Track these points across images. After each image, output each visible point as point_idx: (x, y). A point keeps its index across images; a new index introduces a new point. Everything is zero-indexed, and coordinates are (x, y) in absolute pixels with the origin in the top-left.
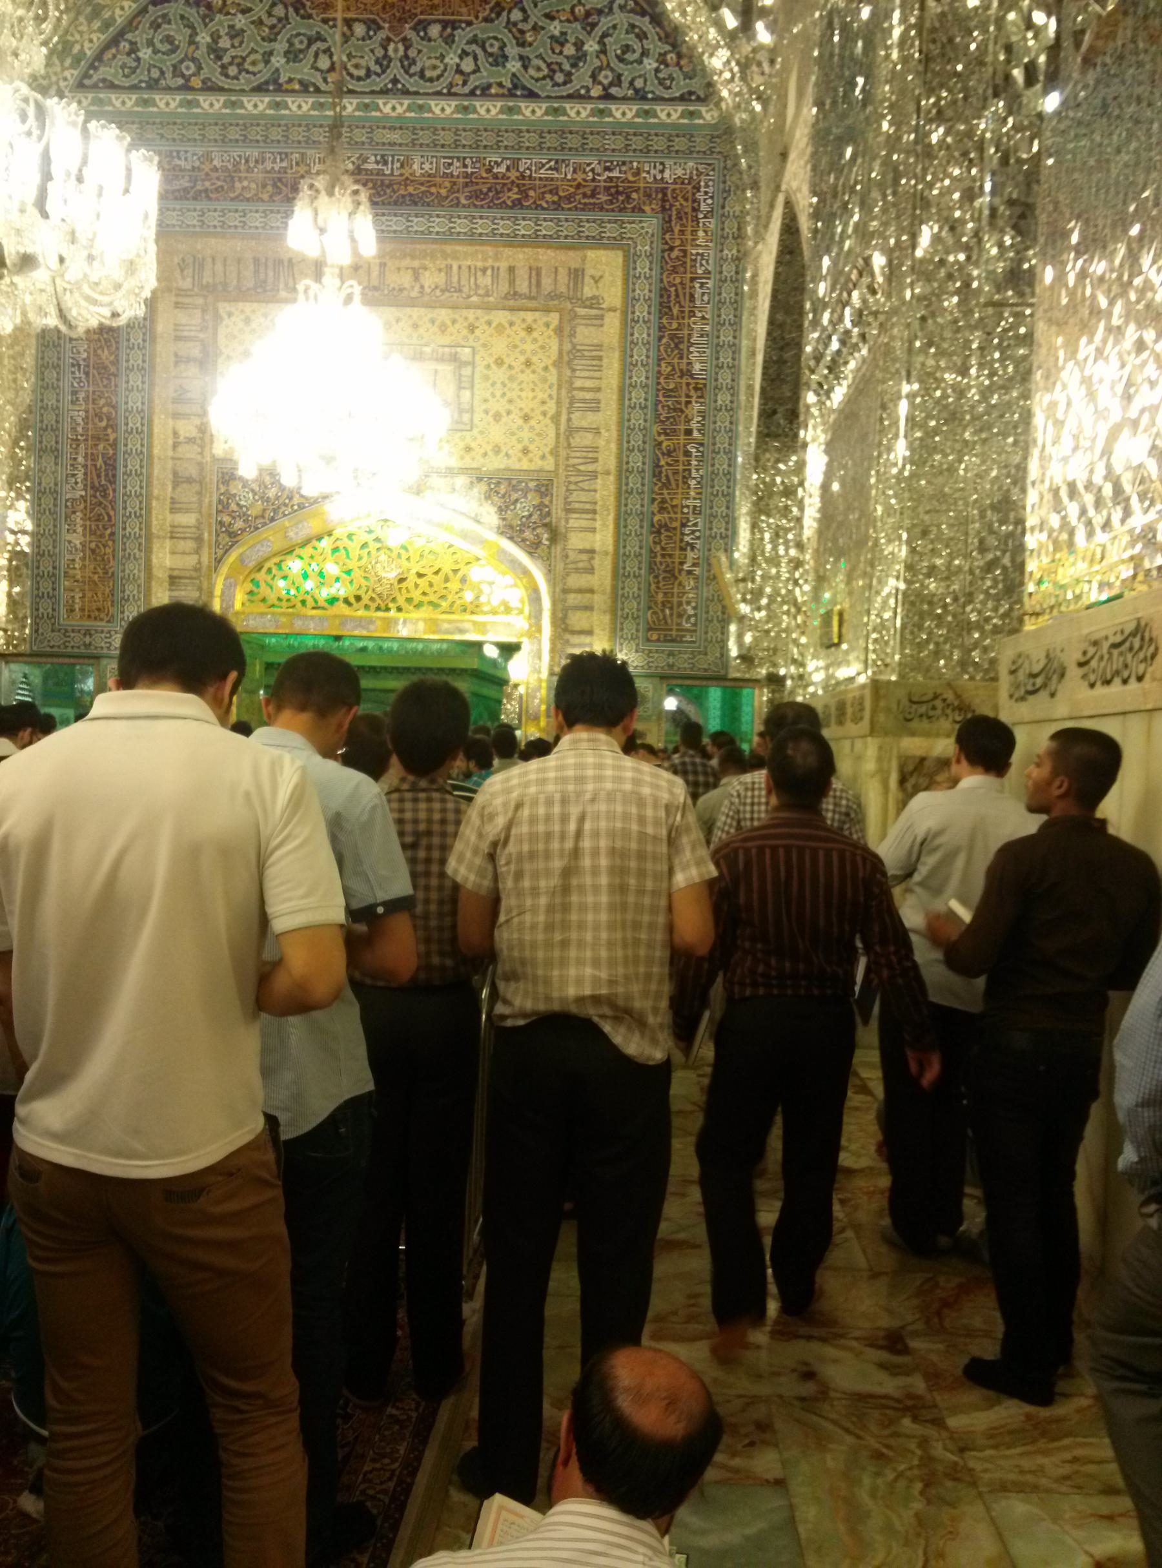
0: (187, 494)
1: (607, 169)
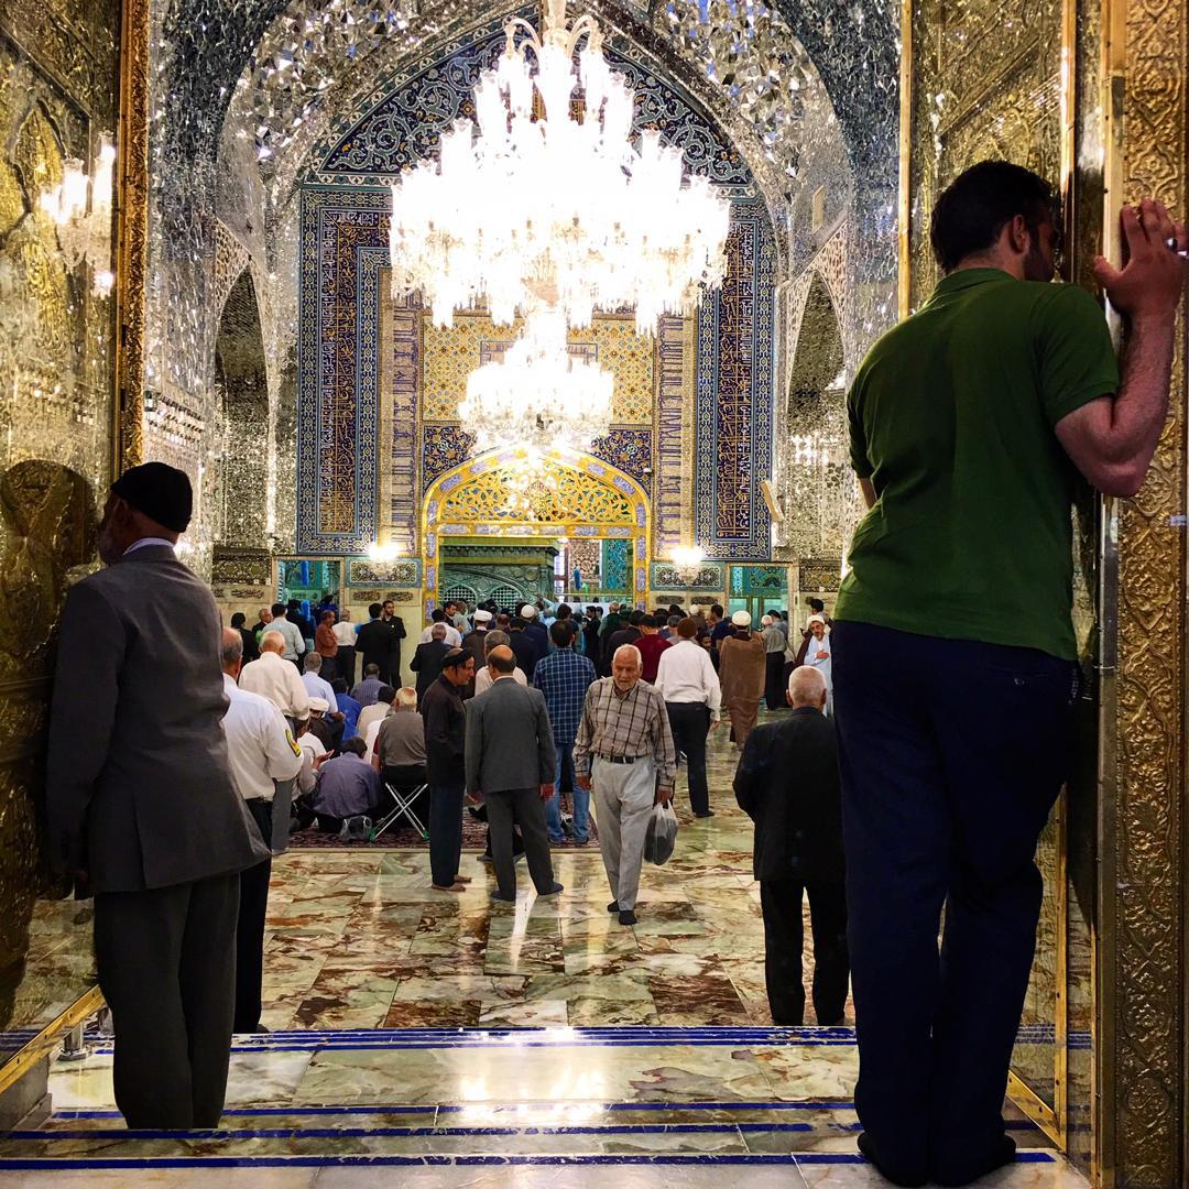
0: (403, 444)
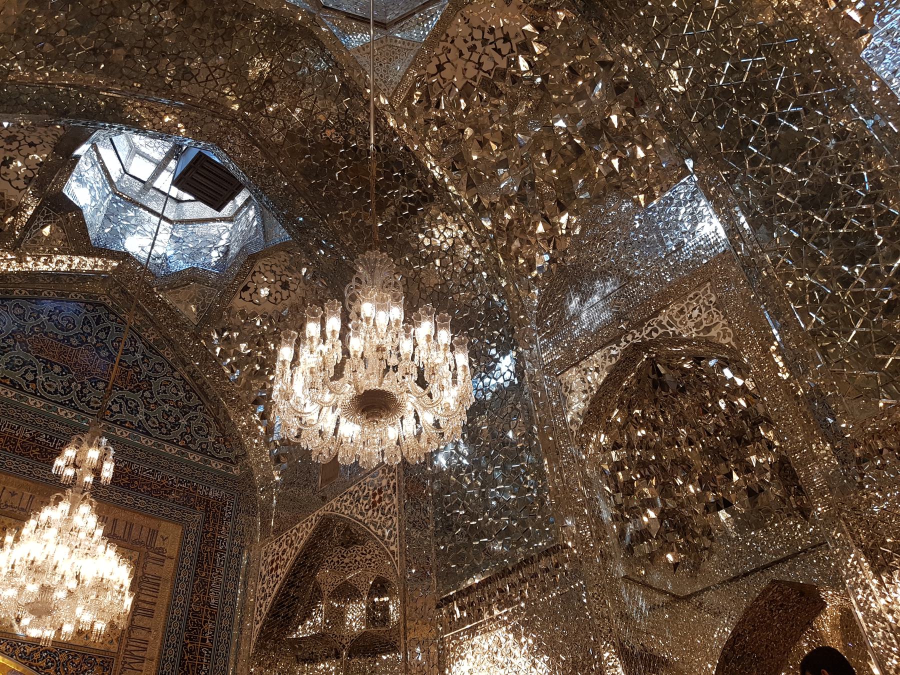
1: (179, 482)
